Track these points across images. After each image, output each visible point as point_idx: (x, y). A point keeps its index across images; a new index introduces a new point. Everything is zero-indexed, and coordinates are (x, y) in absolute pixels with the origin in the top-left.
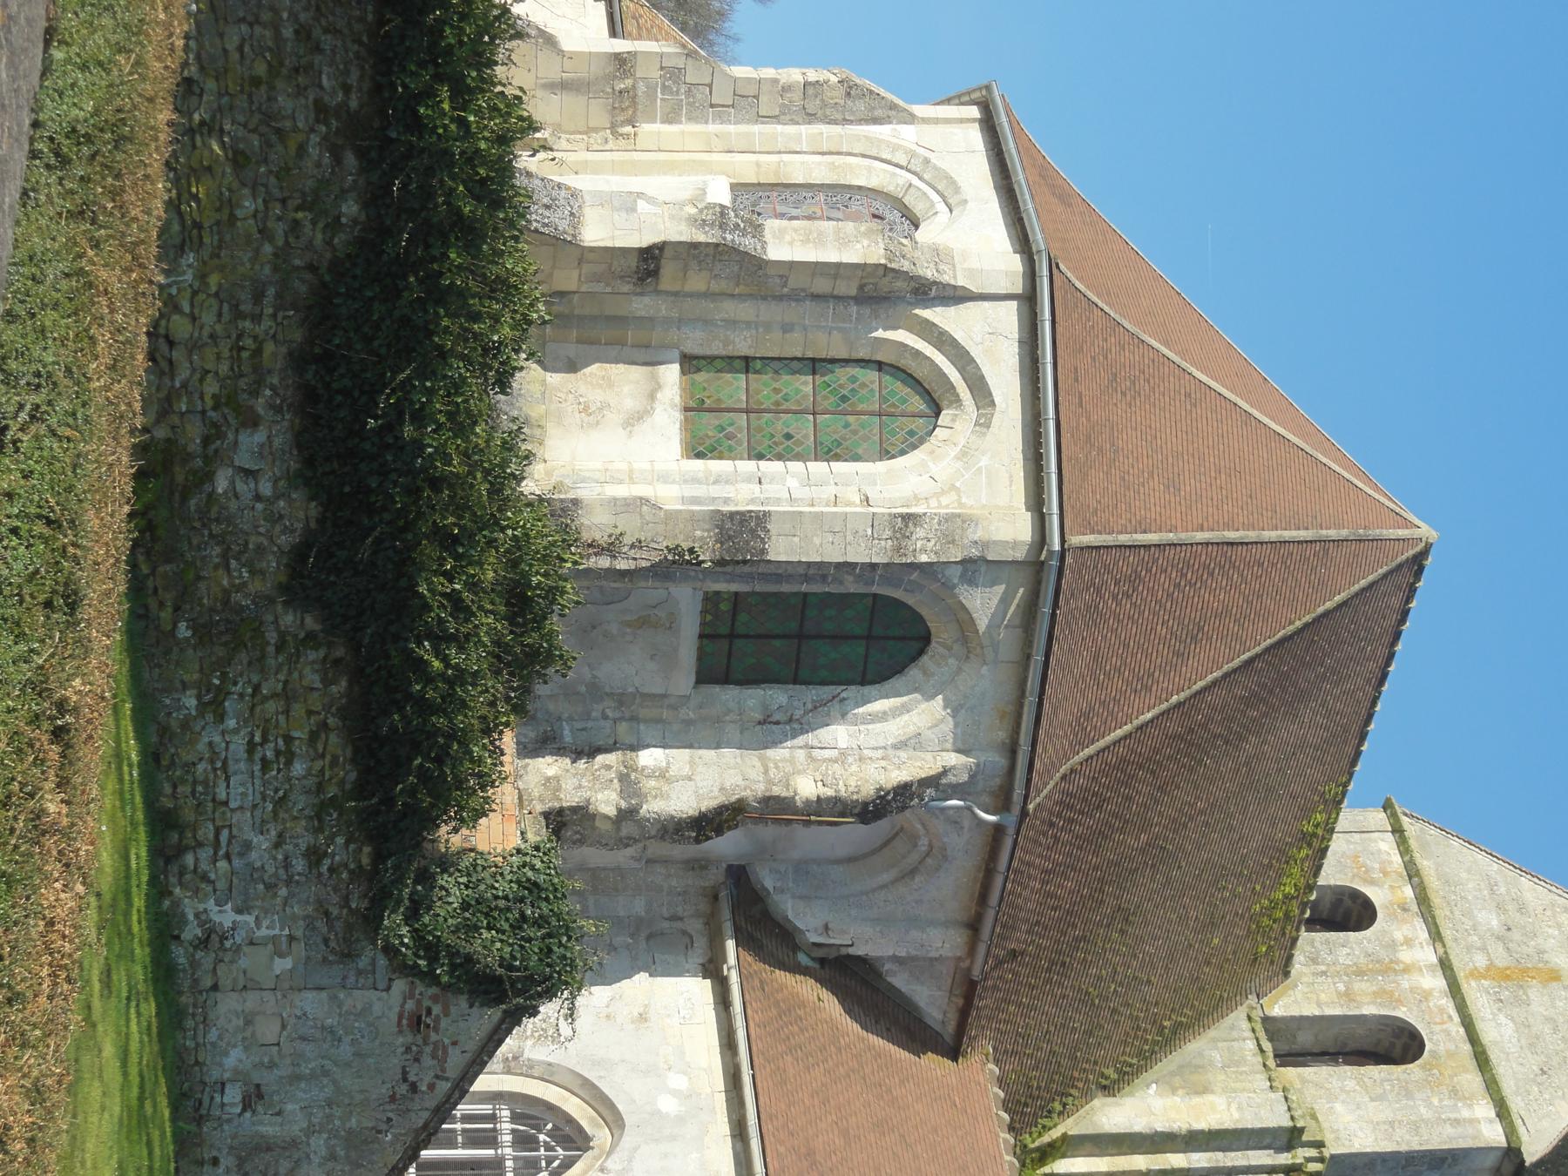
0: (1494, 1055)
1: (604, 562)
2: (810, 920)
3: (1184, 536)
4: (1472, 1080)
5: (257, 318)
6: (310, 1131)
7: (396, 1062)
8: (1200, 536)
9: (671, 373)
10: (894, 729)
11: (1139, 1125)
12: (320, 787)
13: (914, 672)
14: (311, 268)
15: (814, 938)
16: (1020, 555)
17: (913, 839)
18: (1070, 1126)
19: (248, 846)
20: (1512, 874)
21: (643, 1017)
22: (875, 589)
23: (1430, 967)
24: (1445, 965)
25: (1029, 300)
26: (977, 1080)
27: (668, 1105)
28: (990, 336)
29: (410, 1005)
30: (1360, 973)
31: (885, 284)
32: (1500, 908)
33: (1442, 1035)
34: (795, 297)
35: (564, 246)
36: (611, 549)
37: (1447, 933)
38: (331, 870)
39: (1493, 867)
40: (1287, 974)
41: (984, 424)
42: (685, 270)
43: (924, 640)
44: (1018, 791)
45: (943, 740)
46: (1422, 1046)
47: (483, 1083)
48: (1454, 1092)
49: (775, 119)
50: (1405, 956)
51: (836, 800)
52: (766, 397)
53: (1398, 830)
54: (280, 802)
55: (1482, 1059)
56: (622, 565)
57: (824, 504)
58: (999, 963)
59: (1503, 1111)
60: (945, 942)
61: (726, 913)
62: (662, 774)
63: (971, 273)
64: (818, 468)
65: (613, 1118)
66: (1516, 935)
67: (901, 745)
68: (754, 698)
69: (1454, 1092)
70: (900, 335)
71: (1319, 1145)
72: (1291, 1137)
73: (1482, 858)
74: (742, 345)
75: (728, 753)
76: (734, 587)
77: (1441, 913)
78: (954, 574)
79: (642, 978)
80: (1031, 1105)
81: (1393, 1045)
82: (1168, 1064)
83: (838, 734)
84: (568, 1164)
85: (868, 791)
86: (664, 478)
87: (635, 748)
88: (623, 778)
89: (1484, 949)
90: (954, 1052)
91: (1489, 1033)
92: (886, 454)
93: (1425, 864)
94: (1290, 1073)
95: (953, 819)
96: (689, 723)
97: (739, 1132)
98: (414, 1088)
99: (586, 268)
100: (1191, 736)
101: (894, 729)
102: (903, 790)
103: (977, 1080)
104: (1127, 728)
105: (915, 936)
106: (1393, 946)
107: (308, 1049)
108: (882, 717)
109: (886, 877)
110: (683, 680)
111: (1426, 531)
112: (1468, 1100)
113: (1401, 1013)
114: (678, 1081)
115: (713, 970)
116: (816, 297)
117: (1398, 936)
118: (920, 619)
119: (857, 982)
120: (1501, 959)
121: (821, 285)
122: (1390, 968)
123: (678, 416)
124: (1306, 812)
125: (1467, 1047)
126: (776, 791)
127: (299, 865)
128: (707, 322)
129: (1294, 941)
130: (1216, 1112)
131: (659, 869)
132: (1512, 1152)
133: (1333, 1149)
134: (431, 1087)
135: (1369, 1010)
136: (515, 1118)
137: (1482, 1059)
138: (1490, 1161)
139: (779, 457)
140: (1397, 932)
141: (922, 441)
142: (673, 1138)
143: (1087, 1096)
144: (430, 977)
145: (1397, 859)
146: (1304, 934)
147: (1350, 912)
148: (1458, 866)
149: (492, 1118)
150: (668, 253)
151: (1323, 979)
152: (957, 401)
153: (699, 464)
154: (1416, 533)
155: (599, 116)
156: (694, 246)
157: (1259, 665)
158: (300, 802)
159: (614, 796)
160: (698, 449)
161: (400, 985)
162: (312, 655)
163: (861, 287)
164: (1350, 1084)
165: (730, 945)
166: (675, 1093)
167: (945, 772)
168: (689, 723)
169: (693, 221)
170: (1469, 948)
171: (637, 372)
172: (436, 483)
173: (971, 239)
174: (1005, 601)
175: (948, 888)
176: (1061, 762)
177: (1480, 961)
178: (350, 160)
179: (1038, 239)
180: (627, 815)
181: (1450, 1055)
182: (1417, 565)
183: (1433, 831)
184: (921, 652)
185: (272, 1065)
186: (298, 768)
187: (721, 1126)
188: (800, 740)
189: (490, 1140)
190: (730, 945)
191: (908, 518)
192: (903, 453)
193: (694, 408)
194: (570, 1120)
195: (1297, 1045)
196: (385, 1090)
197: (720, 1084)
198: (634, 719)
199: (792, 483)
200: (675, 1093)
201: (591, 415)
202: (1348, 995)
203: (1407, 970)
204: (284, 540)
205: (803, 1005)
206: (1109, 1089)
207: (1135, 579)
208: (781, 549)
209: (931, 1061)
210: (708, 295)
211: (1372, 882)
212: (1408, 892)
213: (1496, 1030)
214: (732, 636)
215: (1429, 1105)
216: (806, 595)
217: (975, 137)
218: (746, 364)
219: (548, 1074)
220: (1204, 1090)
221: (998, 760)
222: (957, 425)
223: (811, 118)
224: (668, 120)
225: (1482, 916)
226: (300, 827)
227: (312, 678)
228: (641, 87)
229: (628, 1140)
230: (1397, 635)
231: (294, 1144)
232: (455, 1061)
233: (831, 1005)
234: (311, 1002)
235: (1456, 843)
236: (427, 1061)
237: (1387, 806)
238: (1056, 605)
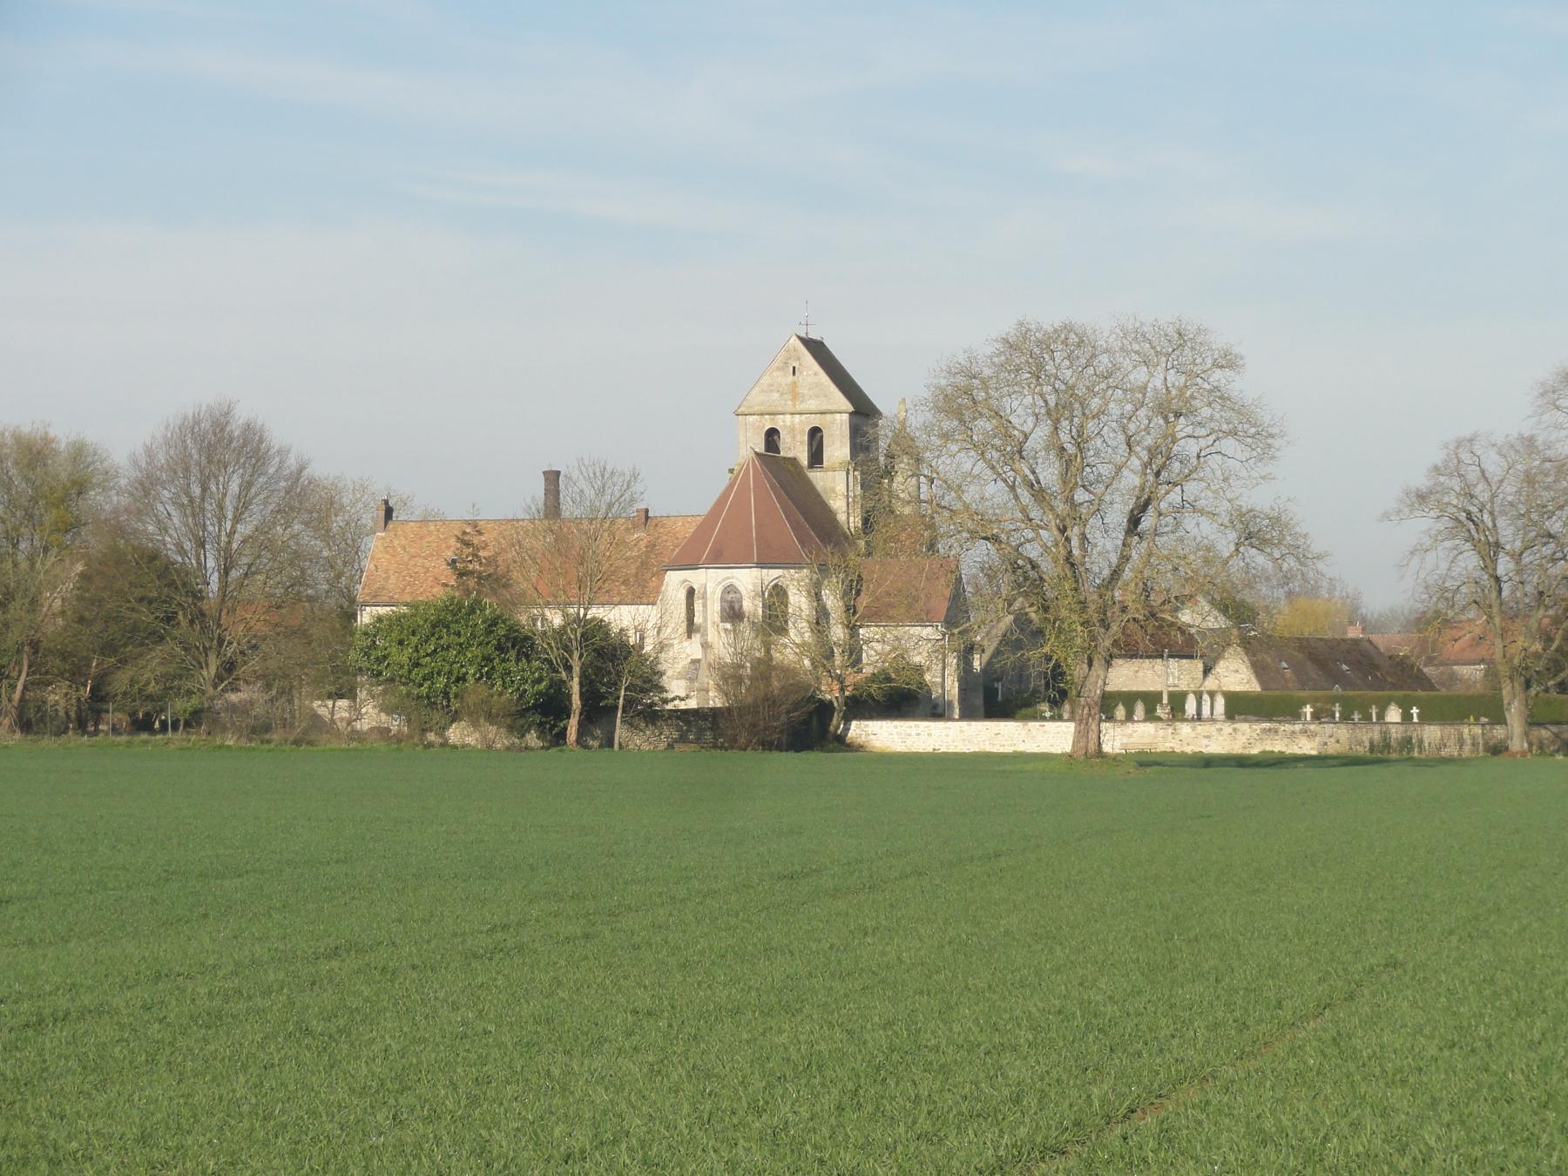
0: (824, 407)
33: (816, 421)
77: (773, 409)
81: (815, 434)
93: (756, 409)
94: (825, 464)
122: (792, 430)
140: (781, 423)
195: (816, 458)
213: (812, 405)
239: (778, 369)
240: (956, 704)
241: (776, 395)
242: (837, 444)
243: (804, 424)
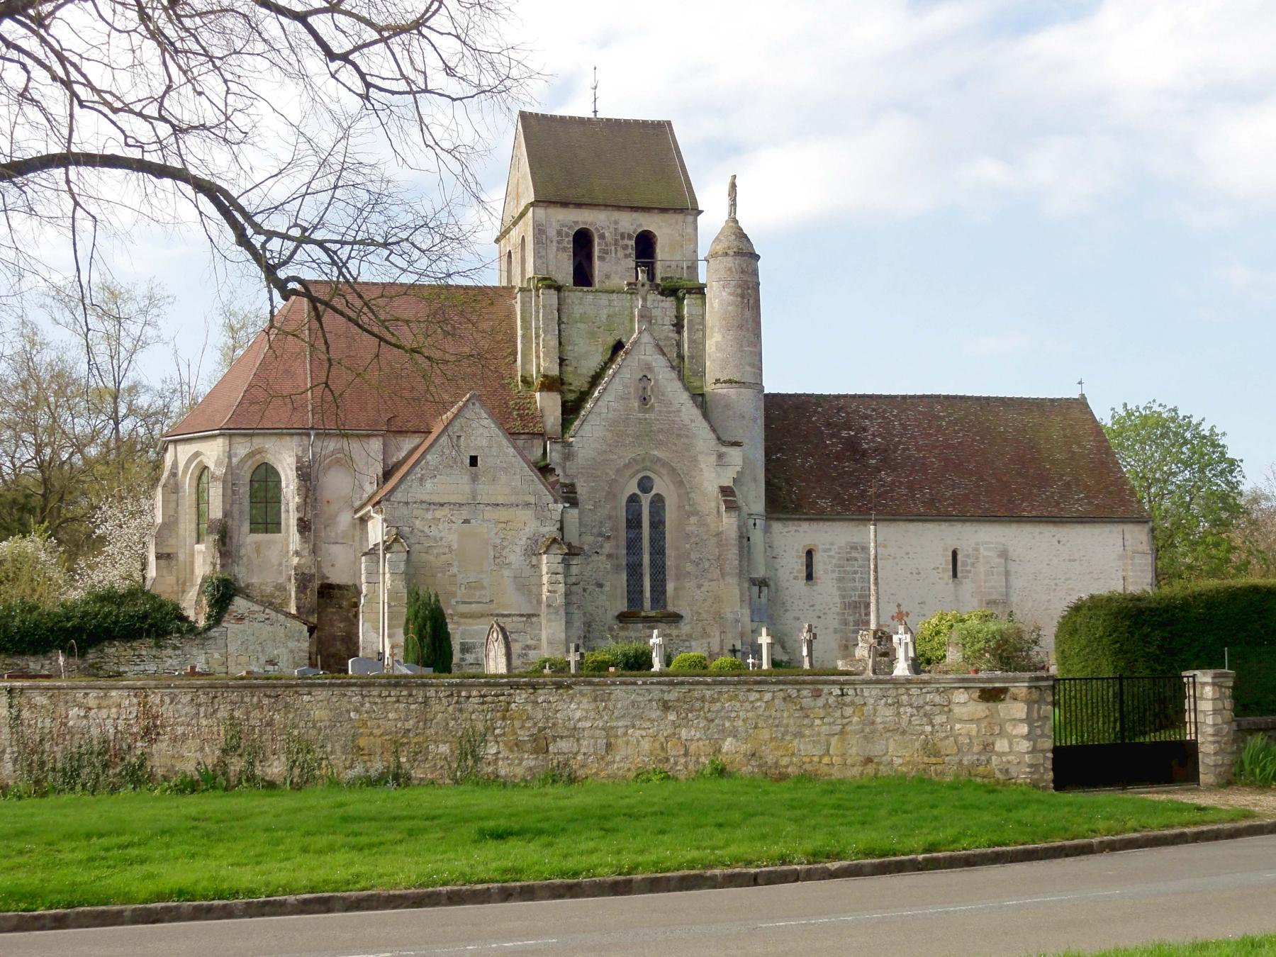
7: (256, 625)
36: (214, 565)
60: (376, 445)
107: (251, 648)
121: (172, 505)
186: (144, 653)
227: (113, 650)
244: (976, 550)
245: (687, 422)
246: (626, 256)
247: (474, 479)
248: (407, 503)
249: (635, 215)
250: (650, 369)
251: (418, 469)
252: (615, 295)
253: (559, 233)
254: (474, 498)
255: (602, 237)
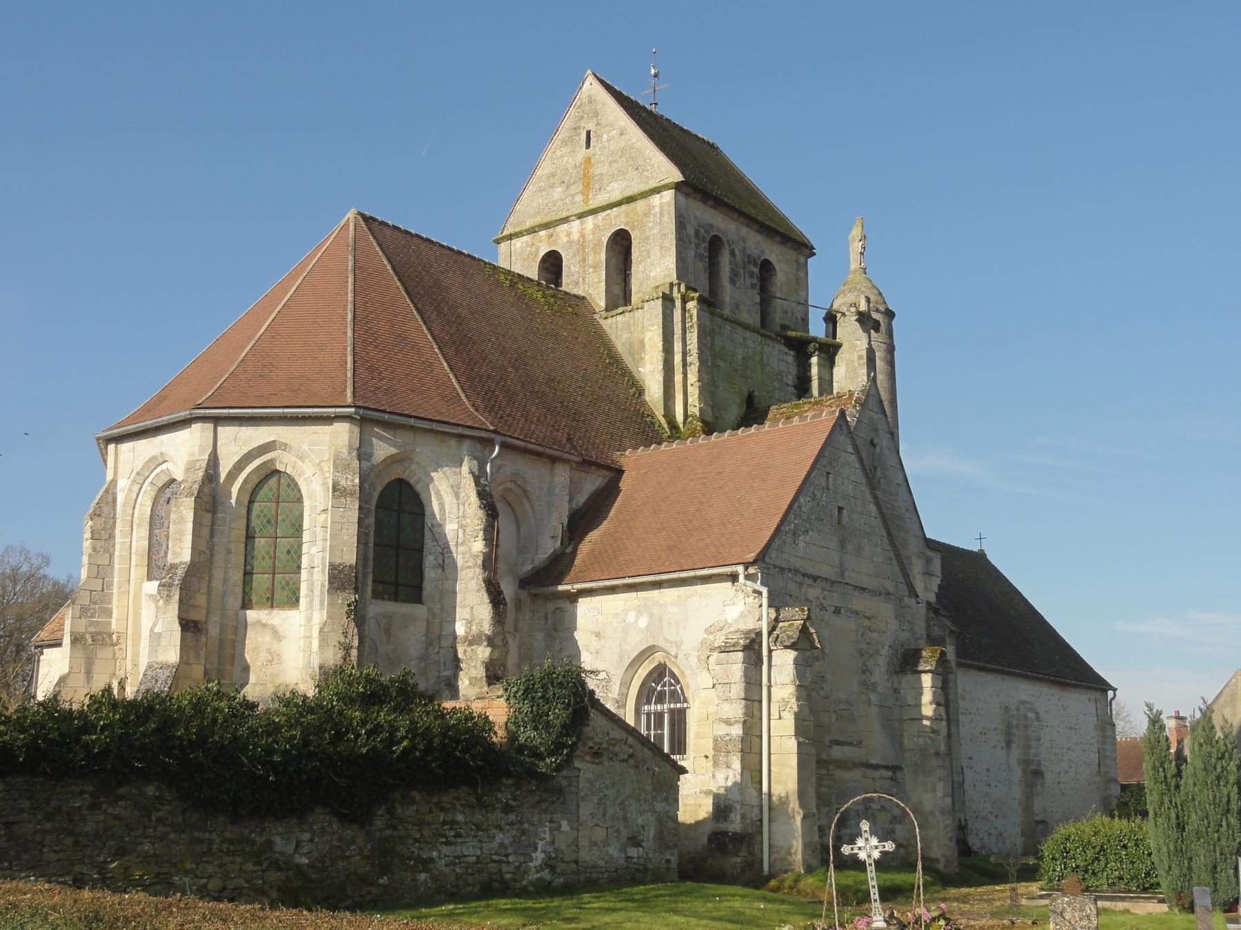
0: (628, 194)
1: (354, 652)
2: (549, 546)
3: (350, 342)
4: (640, 205)
5: (211, 842)
6: (653, 811)
8: (350, 334)
9: (251, 615)
10: (448, 499)
11: (660, 377)
12: (471, 806)
13: (418, 488)
14: (183, 812)
15: (558, 544)
16: (356, 430)
17: (508, 490)
18: (659, 413)
19: (501, 845)
20: (534, 179)
21: (598, 635)
22: (373, 508)
23: (582, 224)
24: (581, 216)
25: (217, 421)
26: (634, 461)
27: (643, 622)
28: (236, 442)
29: (588, 758)
30: (584, 260)
31: (206, 498)
32: (552, 186)
34: (211, 547)
35: (179, 673)
36: (347, 649)
37: (564, 215)
38: (515, 800)
39: (531, 188)
40: (584, 298)
41: (285, 447)
42: (195, 606)
43: (401, 482)
44: (483, 434)
45: (455, 474)
46: (622, 230)
47: (630, 720)
48: (647, 215)
49: (111, 556)
50: (576, 236)
51: (485, 530)
52: (268, 563)
53: (510, 237)
54: (478, 827)
55: (630, 200)
56: (356, 643)
57: (326, 532)
58: (574, 447)
59: (657, 190)
60: (562, 475)
61: (544, 590)
62: (469, 623)
63: (201, 451)
64: (306, 536)
65: (650, 651)
66: (566, 179)
67: (457, 496)
68: (430, 574)
69: (647, 215)
70: (235, 490)
71: (671, 285)
72: (667, 299)
73: (525, 195)
74: (237, 576)
75: (459, 587)
76: (370, 583)
77: (554, 217)
78: (366, 465)
79: (577, 635)
80: (647, 432)
81: (621, 244)
82: (628, 361)
83: (450, 528)
84: (673, 675)
85: (481, 513)
86: (309, 619)
87: (455, 637)
88: (471, 643)
89: (573, 196)
90: (619, 472)
91: (617, 196)
92: (300, 500)
93: (529, 224)
95: (497, 469)
96: (442, 608)
97: (658, 585)
98: (631, 756)
99: (192, 661)
100: (458, 343)
101: (448, 499)
102: (481, 495)
103: (634, 461)
104: (451, 376)
105: (557, 491)
106: (570, 242)
107: (609, 812)
108: (442, 505)
109: (527, 506)
110: (419, 610)
111: (351, 214)
112: (650, 208)
113: (605, 240)
114: (631, 616)
115: (573, 597)
116: (212, 536)
117: (565, 239)
118: (389, 485)
119: (583, 520)
120: (578, 187)
121: (205, 532)
122: (582, 245)
123: (275, 611)
124: (499, 284)
125: (624, 207)
126: (480, 562)
127: (512, 817)
128: (224, 595)
129: (566, 293)
130: (654, 337)
131: (520, 625)
132: (678, 187)
133: (674, 278)
134: (631, 747)
135: (603, 256)
136: (649, 703)
137: (630, 200)
138: (682, 198)
139: (300, 557)
140: (563, 239)
141: (293, 480)
142: (661, 620)
143: (644, 403)
144: (573, 747)
145: (525, 238)
146: (563, 288)
147: (552, 264)
148: (531, 204)
149: (648, 715)
150: (184, 616)
151: (586, 279)
152: (272, 461)
153: (302, 600)
154: (352, 219)
155: (106, 653)
156: (181, 601)
157: (420, 306)
158: (478, 817)
159: (480, 648)
160: (293, 602)
161: (577, 763)
162: (399, 811)
163: (208, 511)
164: (641, 267)
165: (560, 588)
166: (637, 618)
167: (472, 473)
168: (442, 608)
169: (167, 602)
170: (573, 204)
171: (250, 633)
172: (306, 743)
173: (182, 450)
174: (381, 438)
175: (533, 472)
176: (468, 411)
177: (579, 198)
178: (123, 790)
179: (183, 414)
180: (491, 642)
181: (627, 216)
182: (368, 220)
183: (511, 219)
184: (408, 484)
185: (618, 831)
186: (460, 818)
187: (654, 594)
188: (453, 549)
189: (659, 716)
190: (560, 588)
191: (335, 489)
192: (299, 491)
193: (271, 602)
194: (650, 673)
195: (620, 294)
196: (632, 771)
197: (633, 594)
198: (439, 637)
199: (314, 550)
200: (637, 618)
201: (274, 658)
202: (595, 267)
203: (583, 236)
204: (336, 825)
205: (593, 551)
206: (640, 392)
207: (371, 369)
208: (350, 557)
209: (625, 483)
210: (209, 594)
211: (537, 252)
212: (542, 233)
213: (615, 191)
214: (396, 584)
215: (652, 228)
216: (375, 544)
217: (126, 447)
218: (248, 574)
219: (626, 684)
220: (642, 343)
221: (467, 444)
222: (285, 461)
223: (112, 536)
224: (109, 613)
225: (556, 196)
226: (492, 817)
227: (412, 810)
228: (91, 629)
229: (661, 644)
230: (407, 232)
231: (659, 820)
232: (617, 734)
233: (593, 535)
234: (585, 811)
235: (518, 207)
236: (617, 749)
237: (498, 242)
238: (384, 411)
239: (564, 142)
240: (794, 804)
241: (558, 192)
242: (656, 253)
243: (599, 230)
244: (1018, 709)
245: (903, 510)
246: (753, 286)
247: (842, 546)
248: (782, 569)
249: (759, 237)
250: (876, 430)
251: (791, 516)
252: (748, 334)
253: (697, 234)
254: (842, 576)
255: (732, 253)
